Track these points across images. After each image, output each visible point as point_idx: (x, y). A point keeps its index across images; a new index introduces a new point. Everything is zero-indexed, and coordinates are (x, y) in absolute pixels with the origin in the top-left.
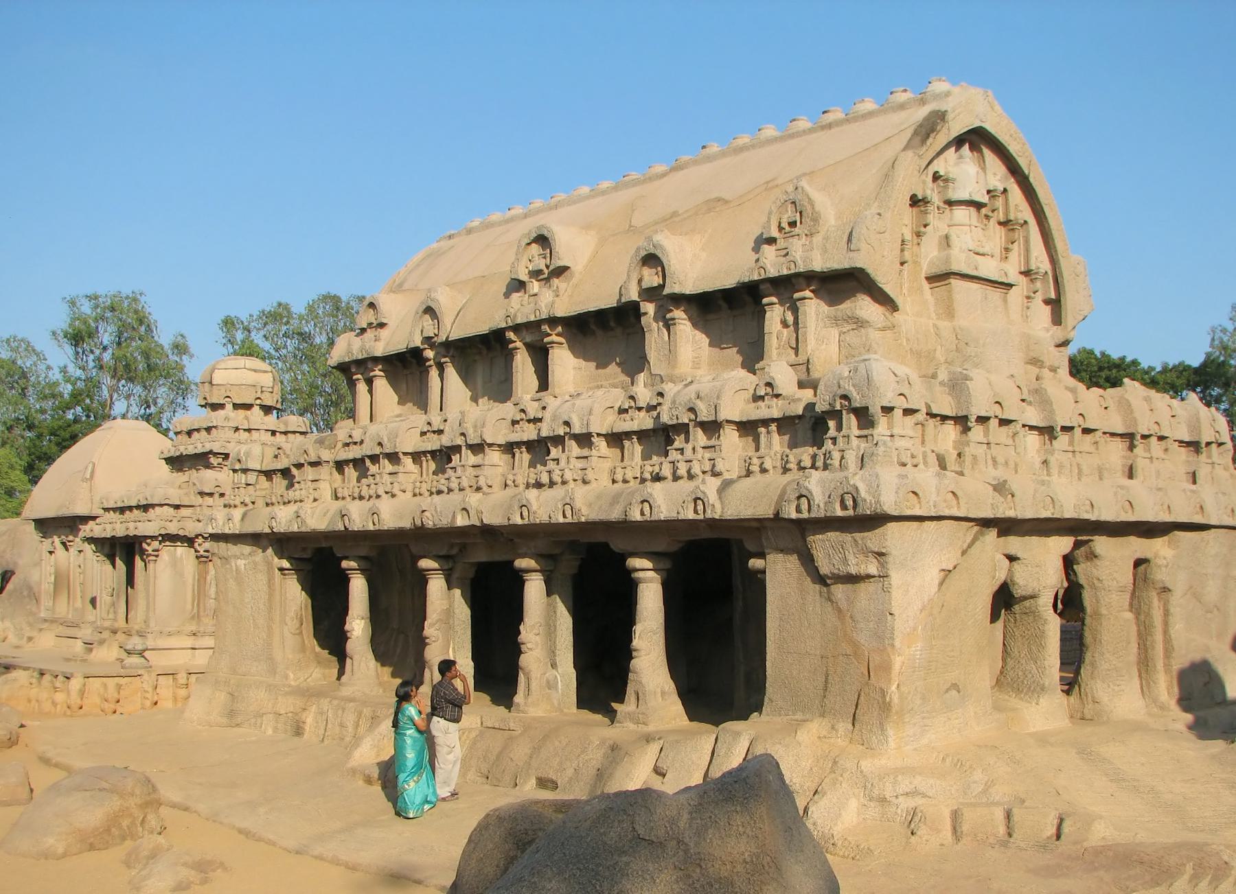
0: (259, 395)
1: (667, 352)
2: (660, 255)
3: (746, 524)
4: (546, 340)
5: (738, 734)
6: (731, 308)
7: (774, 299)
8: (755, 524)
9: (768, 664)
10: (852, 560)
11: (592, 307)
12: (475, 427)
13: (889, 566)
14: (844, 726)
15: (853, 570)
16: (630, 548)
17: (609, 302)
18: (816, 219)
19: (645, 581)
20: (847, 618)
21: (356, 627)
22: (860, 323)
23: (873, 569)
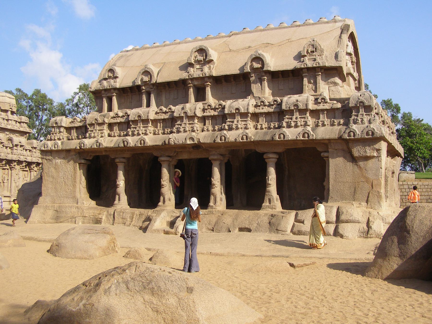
0: (11, 107)
1: (260, 89)
2: (262, 58)
3: (322, 142)
4: (205, 84)
5: (332, 207)
6: (283, 77)
7: (307, 74)
8: (327, 142)
9: (330, 186)
10: (368, 151)
11: (228, 73)
12: (191, 110)
13: (382, 153)
14: (364, 204)
15: (368, 155)
17: (236, 71)
18: (322, 51)
20: (364, 170)
21: (121, 183)
22: (335, 84)
23: (375, 154)
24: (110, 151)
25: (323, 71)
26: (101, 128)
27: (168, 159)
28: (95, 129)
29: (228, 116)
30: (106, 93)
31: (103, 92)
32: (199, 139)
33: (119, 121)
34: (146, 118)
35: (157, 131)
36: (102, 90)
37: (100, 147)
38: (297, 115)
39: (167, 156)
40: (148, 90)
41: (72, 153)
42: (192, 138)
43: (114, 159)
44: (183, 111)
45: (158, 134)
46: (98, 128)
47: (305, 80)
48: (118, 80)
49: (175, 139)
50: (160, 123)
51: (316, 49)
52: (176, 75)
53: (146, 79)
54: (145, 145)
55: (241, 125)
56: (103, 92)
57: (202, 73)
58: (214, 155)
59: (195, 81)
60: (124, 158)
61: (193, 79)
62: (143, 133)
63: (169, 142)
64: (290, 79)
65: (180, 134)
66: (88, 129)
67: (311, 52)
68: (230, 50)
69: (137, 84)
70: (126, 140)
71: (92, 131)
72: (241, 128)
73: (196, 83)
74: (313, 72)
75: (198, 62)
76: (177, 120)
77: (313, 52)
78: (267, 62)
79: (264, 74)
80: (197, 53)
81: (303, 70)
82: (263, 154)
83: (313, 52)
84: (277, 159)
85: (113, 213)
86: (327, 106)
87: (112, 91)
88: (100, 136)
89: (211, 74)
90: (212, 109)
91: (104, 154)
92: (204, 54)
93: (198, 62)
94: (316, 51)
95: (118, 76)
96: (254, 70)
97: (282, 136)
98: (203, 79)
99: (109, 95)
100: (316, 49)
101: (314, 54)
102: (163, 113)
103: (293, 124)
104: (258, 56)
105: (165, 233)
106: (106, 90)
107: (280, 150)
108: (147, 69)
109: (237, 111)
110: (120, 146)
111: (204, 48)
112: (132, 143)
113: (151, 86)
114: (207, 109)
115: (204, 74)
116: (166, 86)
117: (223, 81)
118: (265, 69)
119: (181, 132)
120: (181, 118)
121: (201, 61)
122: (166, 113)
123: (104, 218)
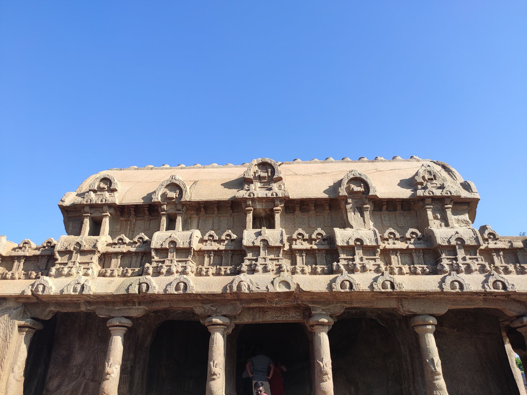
2: (365, 179)
16: (419, 312)
19: (428, 331)
21: (115, 370)
24: (97, 303)
25: (452, 203)
26: (86, 259)
27: (227, 321)
28: (73, 260)
29: (340, 250)
30: (92, 211)
31: (87, 209)
32: (298, 285)
33: (125, 250)
34: (186, 245)
35: (204, 269)
36: (87, 205)
37: (84, 293)
39: (224, 316)
40: (172, 211)
41: (11, 304)
42: (287, 284)
43: (105, 320)
44: (260, 238)
45: (207, 275)
46: (78, 258)
47: (430, 213)
48: (116, 194)
49: (251, 282)
50: (209, 257)
51: (434, 176)
53: (172, 194)
54: (188, 291)
55: (370, 265)
56: (87, 209)
57: (271, 192)
59: (257, 203)
60: (127, 317)
61: (253, 200)
62: (177, 272)
63: (239, 287)
64: (408, 210)
65: (256, 275)
66: (57, 260)
67: (429, 179)
68: (296, 174)
69: (156, 200)
70: (145, 281)
71: (66, 264)
72: (370, 270)
73: (258, 206)
75: (260, 178)
76: (247, 251)
77: (432, 179)
78: (373, 185)
79: (367, 201)
80: (257, 168)
81: (426, 200)
82: (415, 315)
83: (432, 179)
84: (436, 326)
86: (500, 245)
87: (105, 208)
88: (81, 273)
89: (286, 194)
91: (83, 309)
92: (270, 170)
93: (260, 178)
94: (435, 179)
95: (117, 188)
96: (351, 193)
97: (457, 284)
98: (272, 201)
99: (96, 215)
100: (434, 176)
101: (434, 181)
102: (215, 241)
103: (463, 267)
104: (358, 176)
106: (93, 206)
107: (442, 311)
108: (174, 181)
109: (358, 243)
110: (131, 291)
112: (157, 287)
113: (180, 207)
114: (296, 240)
115: (275, 194)
116: (202, 209)
117: (298, 208)
119: (258, 271)
120: (255, 249)
121: (264, 178)
122: (220, 241)
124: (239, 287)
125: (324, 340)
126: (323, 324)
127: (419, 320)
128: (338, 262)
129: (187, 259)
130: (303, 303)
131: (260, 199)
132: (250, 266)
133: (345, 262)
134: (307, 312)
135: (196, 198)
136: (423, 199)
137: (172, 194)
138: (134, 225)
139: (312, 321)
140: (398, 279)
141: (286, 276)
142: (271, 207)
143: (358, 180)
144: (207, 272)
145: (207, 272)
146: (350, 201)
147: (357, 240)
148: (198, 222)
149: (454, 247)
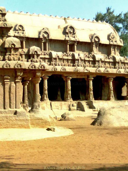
38: (120, 64)
44: (79, 57)
51: (114, 37)
52: (61, 37)
53: (46, 35)
58: (91, 77)
61: (70, 41)
74: (115, 46)
85: (50, 104)
89: (79, 40)
90: (87, 57)
96: (95, 41)
98: (74, 42)
100: (114, 37)
103: (120, 67)
104: (97, 36)
105: (93, 111)
107: (115, 77)
111: (73, 26)
118: (100, 42)
120: (78, 60)
121: (72, 32)
123: (46, 107)
124: (77, 70)
125: (91, 82)
126: (91, 79)
127: (110, 79)
128: (96, 64)
129: (61, 61)
130: (88, 74)
131: (72, 41)
132: (77, 64)
133: (98, 65)
134: (88, 77)
135: (53, 38)
136: (111, 45)
137: (46, 35)
138: (30, 43)
139: (89, 79)
140: (109, 69)
141: (87, 68)
142: (73, 43)
143: (97, 37)
144: (66, 65)
145: (66, 65)
146: (94, 44)
147: (100, 59)
148: (51, 44)
149: (119, 62)
